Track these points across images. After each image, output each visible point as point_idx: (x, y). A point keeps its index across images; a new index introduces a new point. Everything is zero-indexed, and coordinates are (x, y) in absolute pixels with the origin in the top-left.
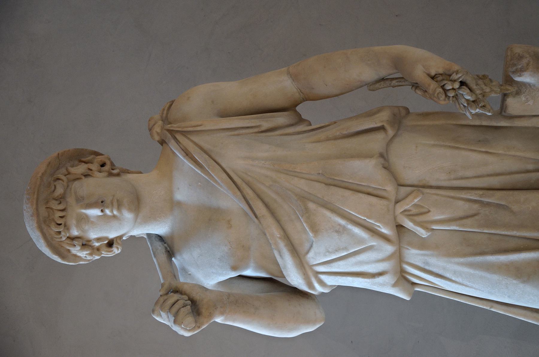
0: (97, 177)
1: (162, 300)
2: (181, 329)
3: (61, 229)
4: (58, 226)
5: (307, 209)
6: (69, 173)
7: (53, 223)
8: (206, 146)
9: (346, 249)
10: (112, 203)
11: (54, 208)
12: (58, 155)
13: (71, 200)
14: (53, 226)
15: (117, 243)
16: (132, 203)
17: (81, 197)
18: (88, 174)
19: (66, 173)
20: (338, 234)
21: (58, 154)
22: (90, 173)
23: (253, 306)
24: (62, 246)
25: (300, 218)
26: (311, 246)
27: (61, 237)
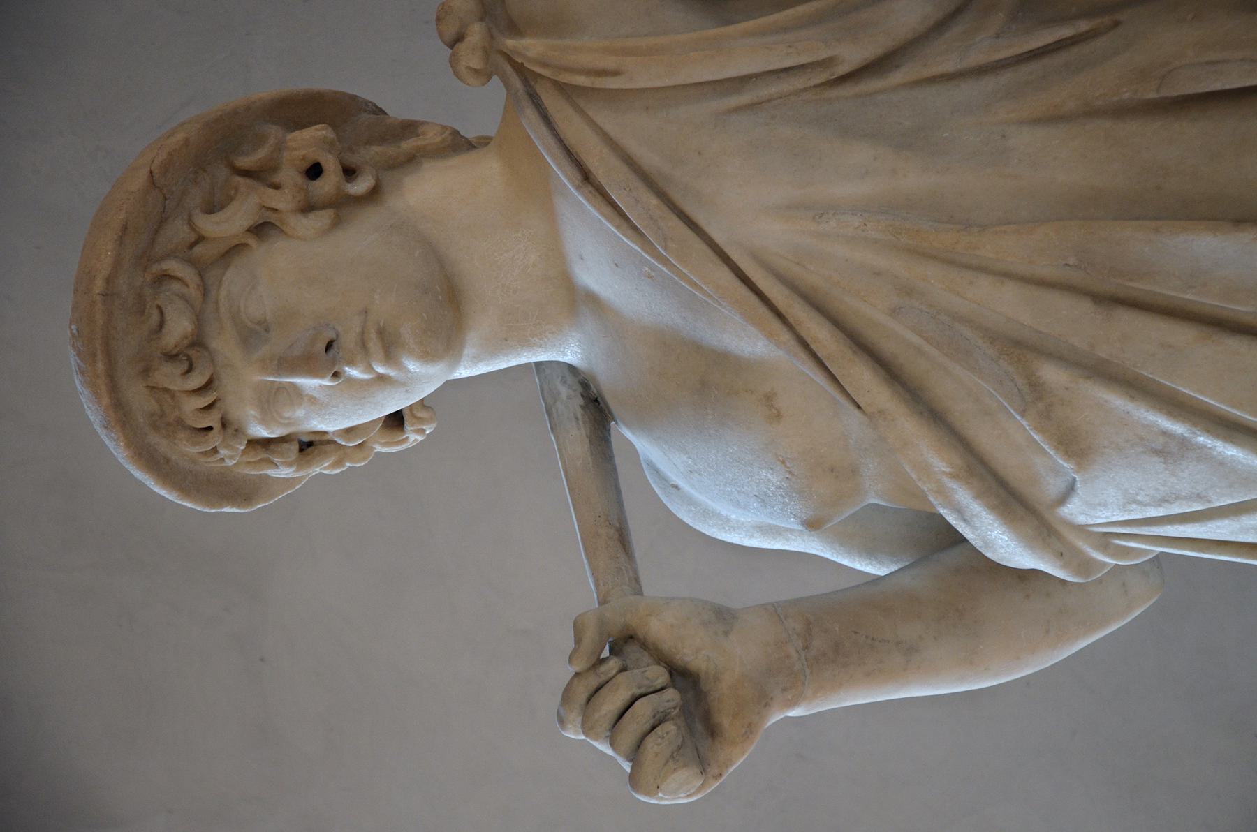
0: (298, 238)
1: (582, 692)
3: (215, 439)
5: (1037, 389)
6: (200, 239)
8: (649, 158)
9: (1199, 497)
10: (363, 345)
11: (176, 388)
12: (152, 176)
13: (224, 344)
15: (414, 421)
16: (429, 333)
17: (259, 323)
18: (268, 220)
19: (193, 237)
20: (1162, 460)
21: (151, 172)
22: (273, 218)
23: (898, 643)
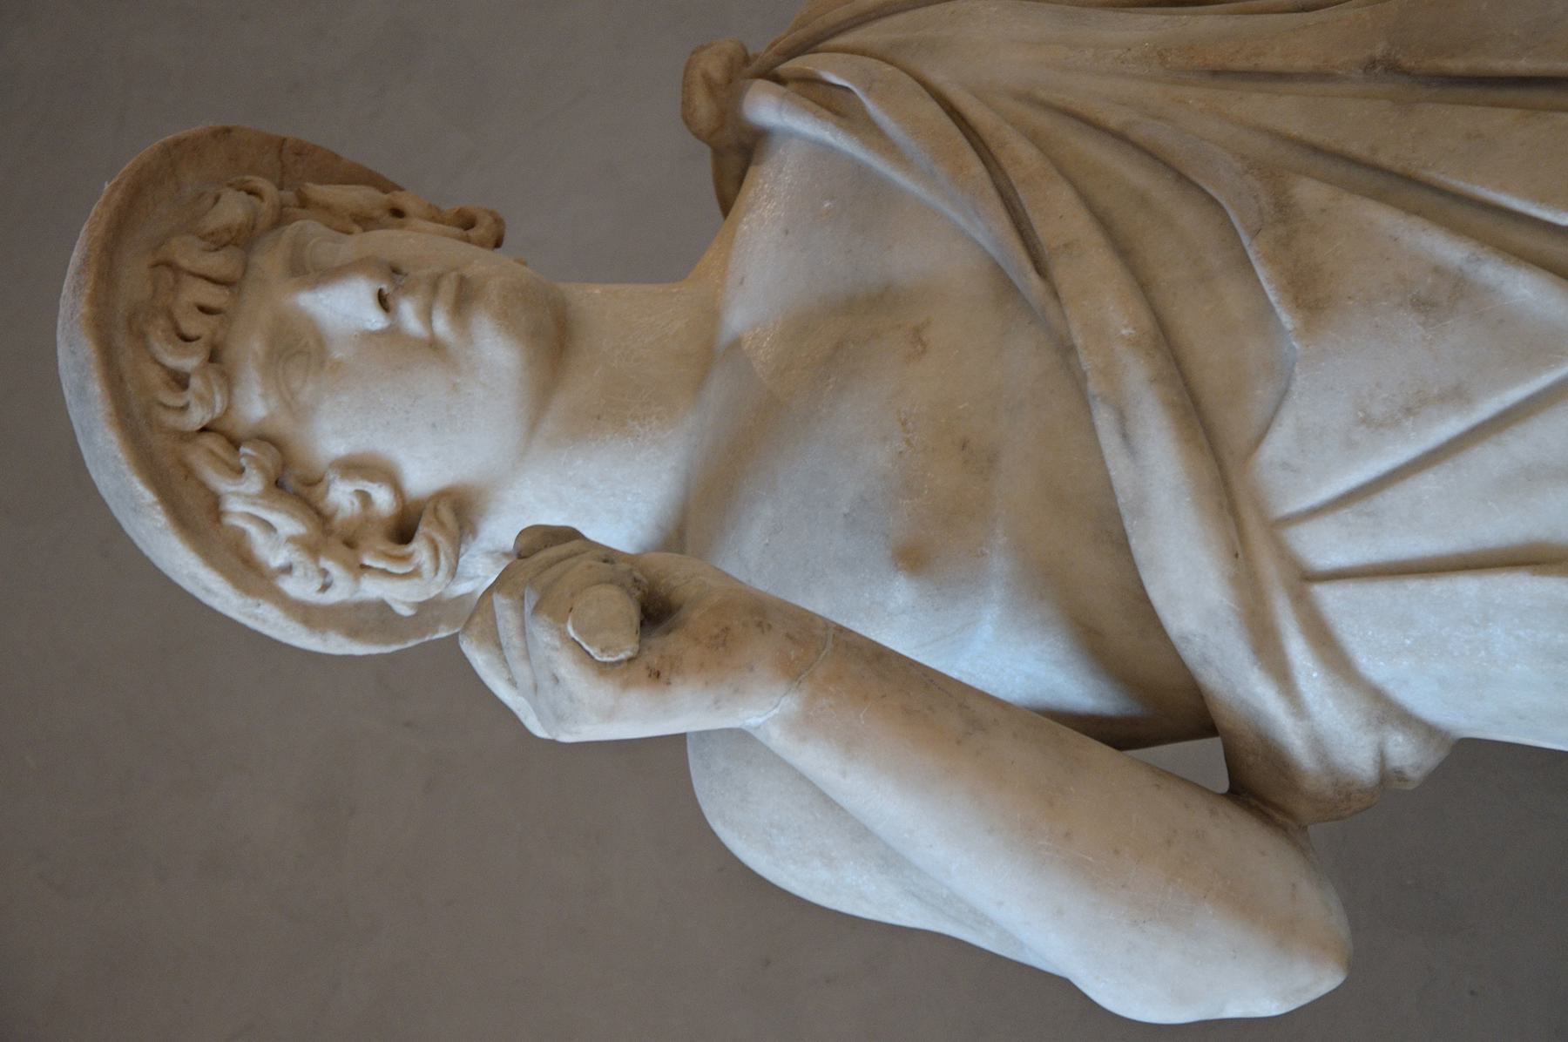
2: (558, 644)
4: (181, 342)
5: (1284, 209)
7: (162, 322)
9: (1458, 396)
10: (435, 285)
11: (184, 263)
14: (160, 334)
16: (520, 295)
24: (189, 472)
25: (1245, 240)
26: (1284, 395)
27: (184, 409)
